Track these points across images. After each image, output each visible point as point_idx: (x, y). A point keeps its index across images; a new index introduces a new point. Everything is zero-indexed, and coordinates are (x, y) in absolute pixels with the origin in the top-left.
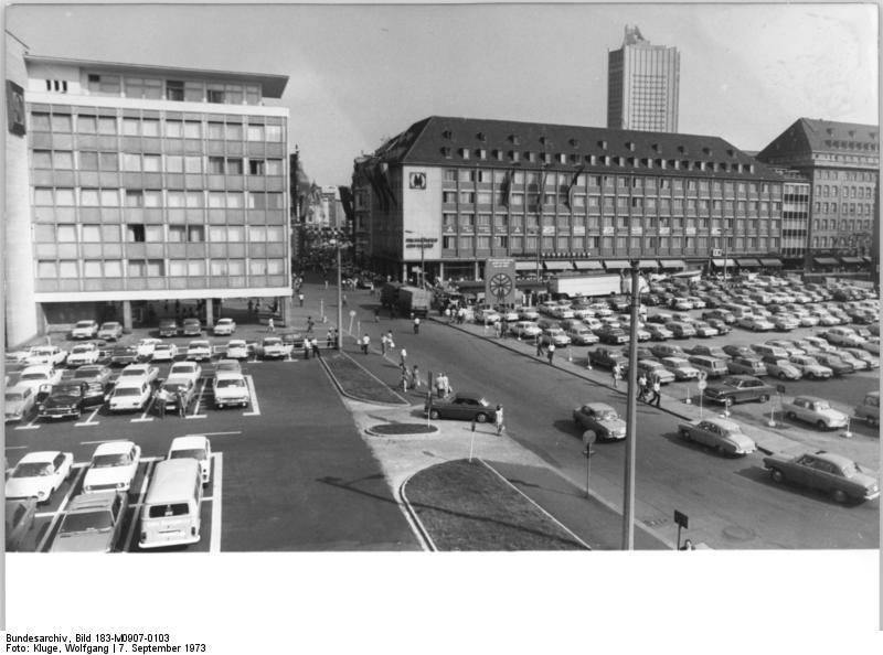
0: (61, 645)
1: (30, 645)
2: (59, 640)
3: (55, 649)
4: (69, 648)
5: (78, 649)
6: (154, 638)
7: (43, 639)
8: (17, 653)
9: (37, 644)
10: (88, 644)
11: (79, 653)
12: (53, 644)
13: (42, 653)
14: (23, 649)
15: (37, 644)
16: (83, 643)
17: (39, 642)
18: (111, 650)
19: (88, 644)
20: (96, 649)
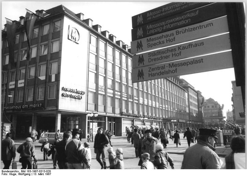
0: (17, 173)
1: (8, 173)
2: (17, 172)
3: (15, 174)
5: (22, 174)
6: (42, 171)
7: (12, 172)
8: (5, 175)
9: (10, 173)
10: (25, 173)
11: (22, 175)
12: (15, 173)
13: (12, 175)
15: (10, 173)
16: (23, 173)
17: (11, 172)
18: (31, 175)
19: (25, 173)
20: (27, 174)
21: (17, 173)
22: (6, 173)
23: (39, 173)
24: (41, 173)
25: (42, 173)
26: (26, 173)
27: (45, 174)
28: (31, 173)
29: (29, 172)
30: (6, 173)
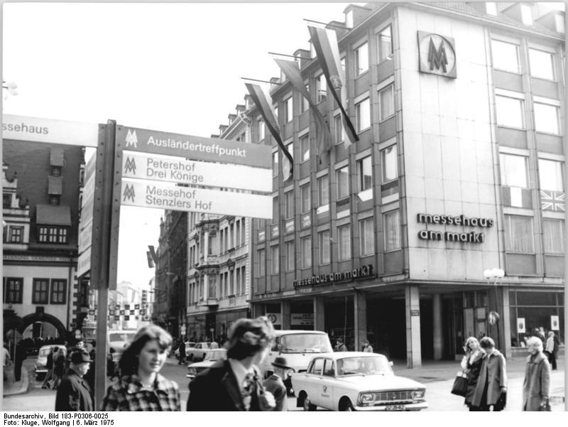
0: (39, 421)
1: (19, 421)
2: (38, 417)
3: (36, 423)
4: (45, 423)
7: (28, 417)
9: (24, 420)
12: (34, 420)
14: (15, 423)
15: (24, 420)
19: (57, 420)
20: (62, 423)
21: (39, 421)
22: (14, 420)
23: (87, 421)
24: (89, 419)
25: (93, 419)
26: (61, 419)
27: (99, 423)
28: (71, 420)
29: (66, 415)
30: (14, 420)
